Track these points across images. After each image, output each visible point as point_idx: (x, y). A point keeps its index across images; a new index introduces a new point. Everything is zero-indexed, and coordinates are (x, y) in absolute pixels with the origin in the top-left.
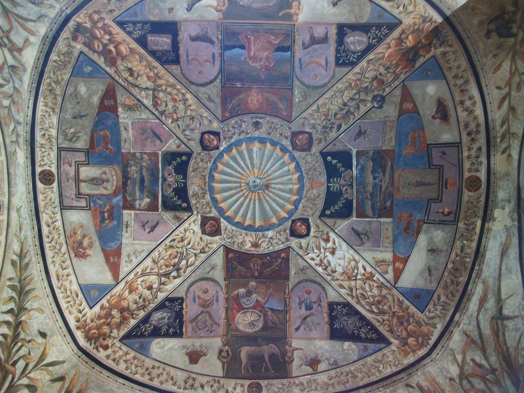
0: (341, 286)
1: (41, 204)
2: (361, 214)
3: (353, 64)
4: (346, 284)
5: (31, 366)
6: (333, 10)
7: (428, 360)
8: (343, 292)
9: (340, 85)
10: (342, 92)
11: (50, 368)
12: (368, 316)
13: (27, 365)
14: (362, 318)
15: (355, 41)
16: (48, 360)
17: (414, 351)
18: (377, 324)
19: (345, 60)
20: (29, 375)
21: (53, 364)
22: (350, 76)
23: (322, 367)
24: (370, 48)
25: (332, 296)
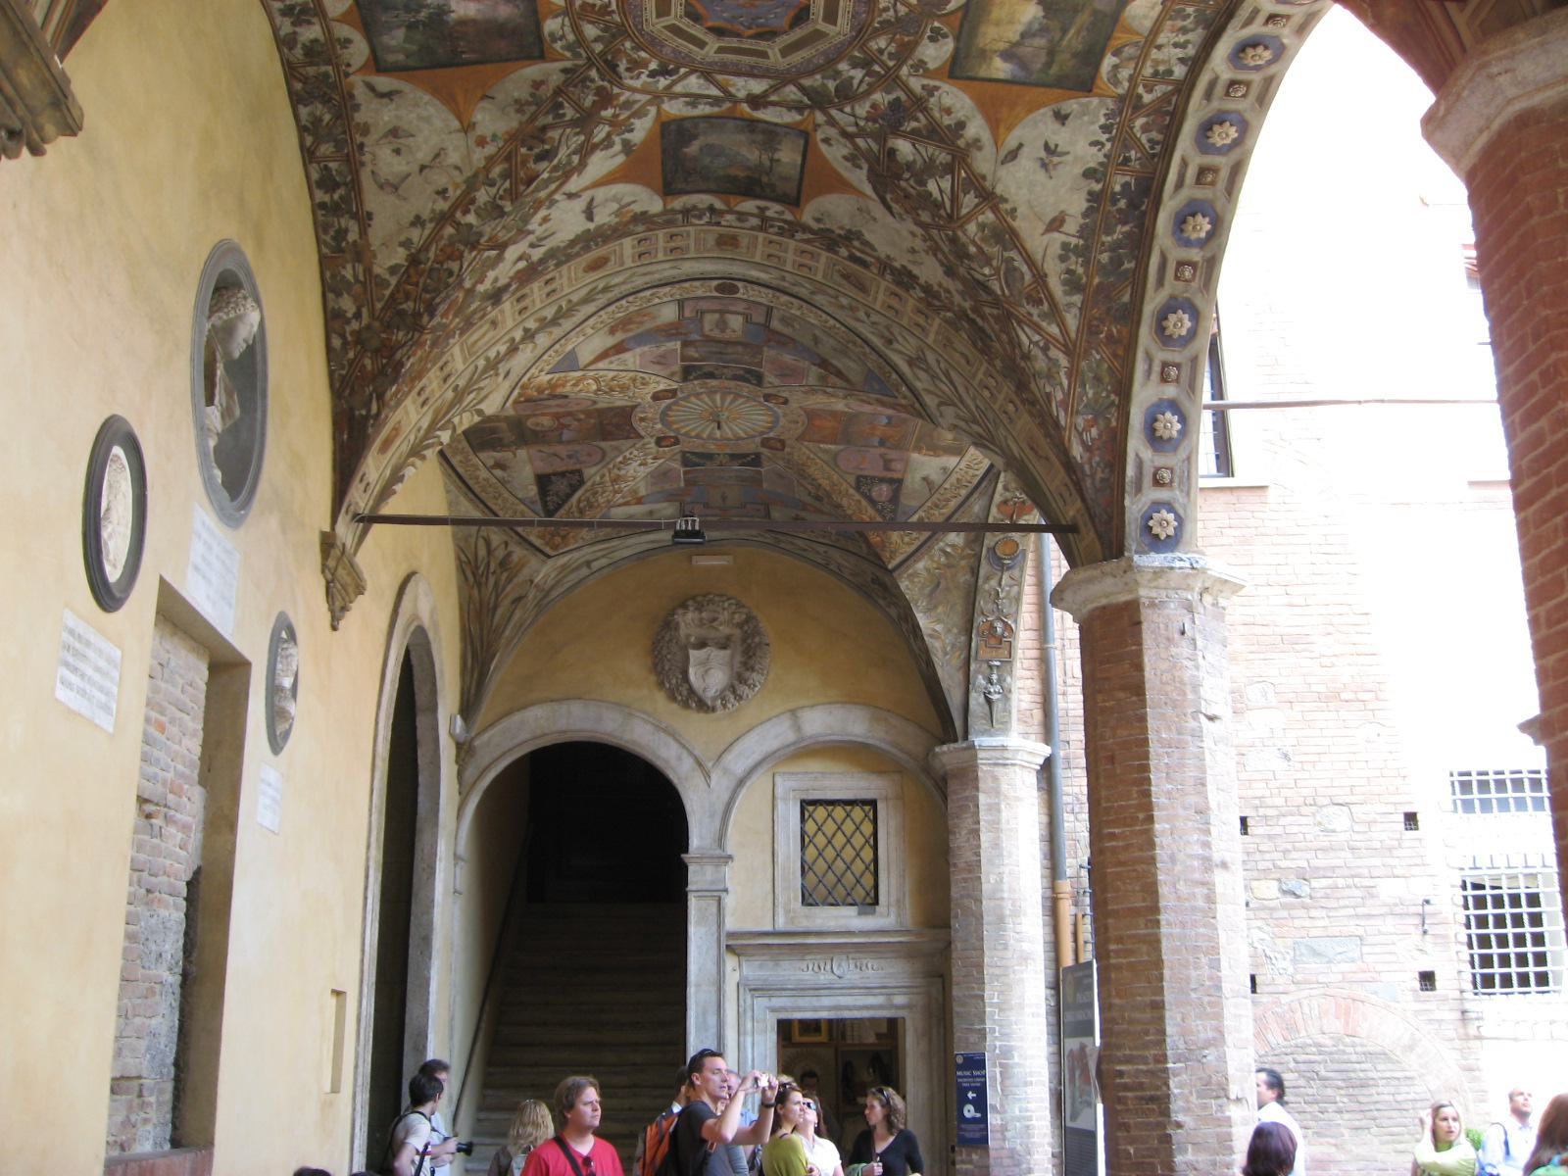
0: (603, 476)
1: (687, 285)
2: (685, 473)
3: (858, 488)
4: (607, 478)
6: (918, 477)
7: (543, 557)
8: (597, 478)
9: (835, 477)
10: (828, 478)
12: (574, 500)
14: (569, 496)
15: (882, 492)
17: (547, 544)
18: (566, 507)
19: (862, 483)
22: (845, 485)
23: (498, 472)
24: (873, 502)
25: (589, 472)
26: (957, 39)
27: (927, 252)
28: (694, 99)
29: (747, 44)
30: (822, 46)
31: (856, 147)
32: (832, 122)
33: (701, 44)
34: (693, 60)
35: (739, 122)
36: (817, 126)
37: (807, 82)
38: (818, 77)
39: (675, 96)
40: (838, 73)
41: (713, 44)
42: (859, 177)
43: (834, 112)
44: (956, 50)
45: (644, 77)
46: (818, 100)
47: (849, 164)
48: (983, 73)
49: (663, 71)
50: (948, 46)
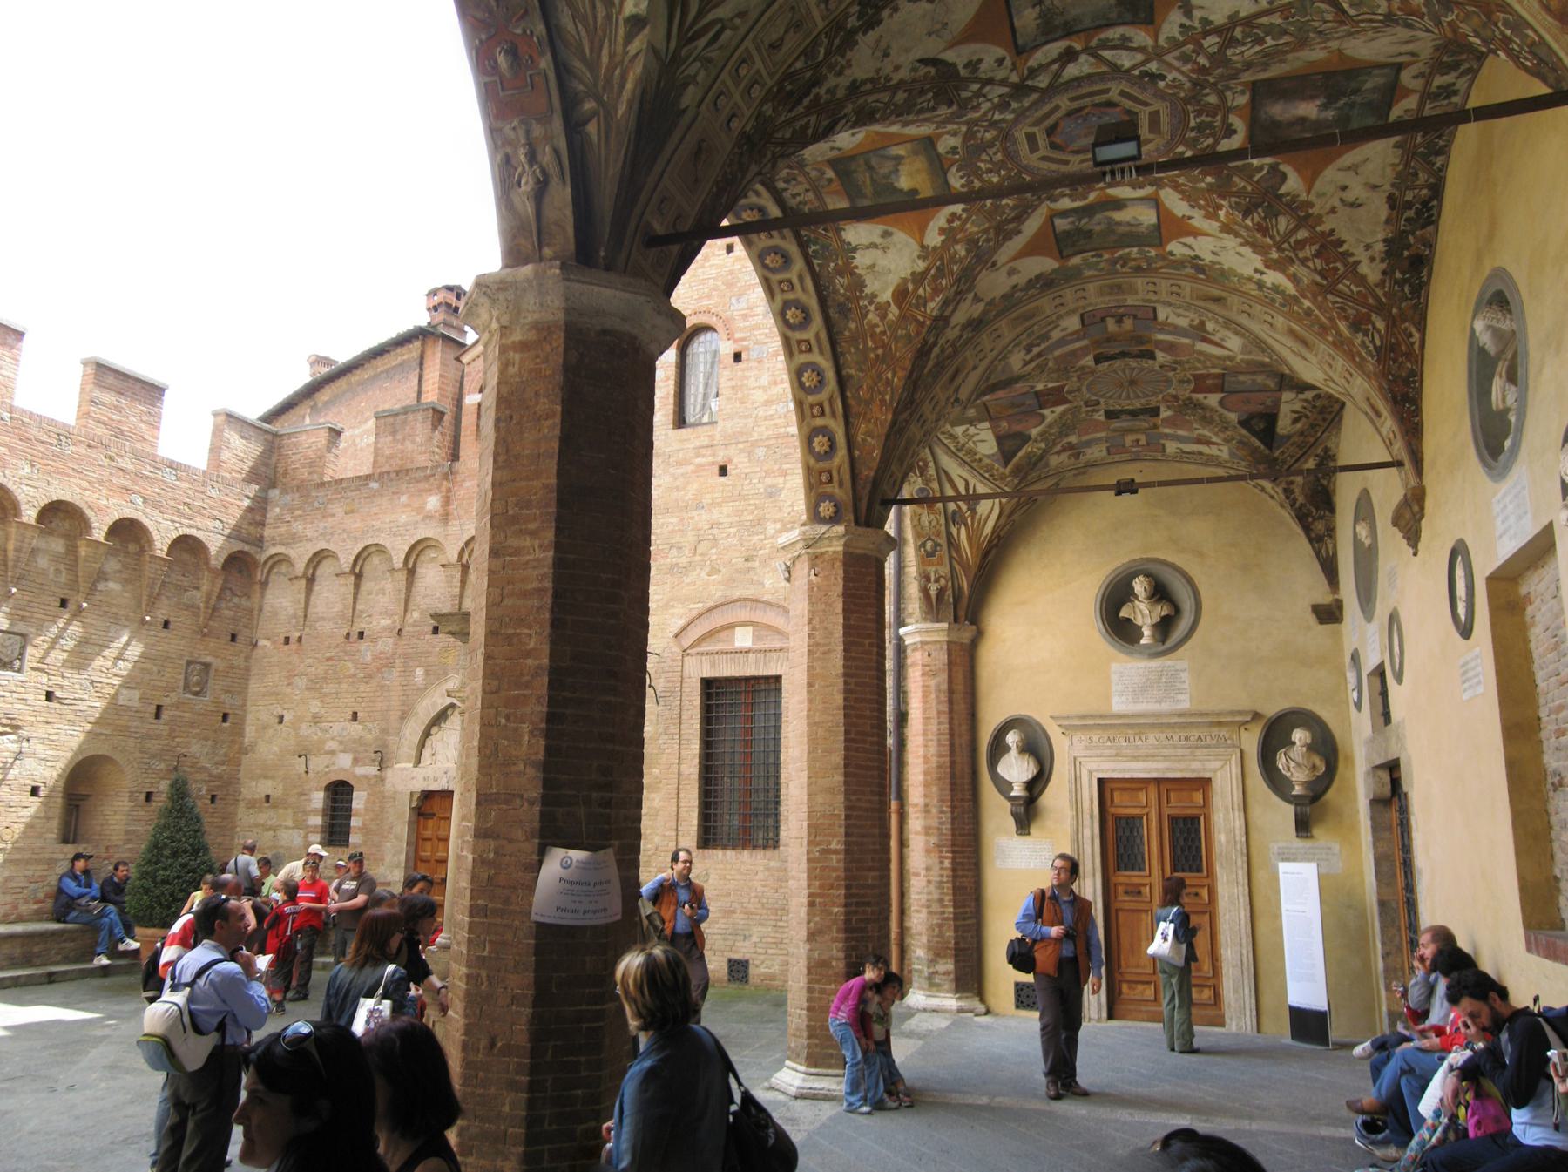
26: (938, 155)
27: (878, 71)
28: (1124, 44)
29: (1087, 101)
30: (1030, 120)
31: (977, 80)
32: (1003, 82)
33: (1123, 94)
34: (1129, 80)
35: (1080, 27)
36: (1014, 68)
37: (1035, 96)
38: (1026, 104)
39: (1141, 49)
40: (1014, 111)
41: (1114, 95)
42: (957, 57)
43: (1005, 90)
44: (935, 150)
45: (1170, 77)
46: (1020, 90)
47: (975, 58)
48: (908, 145)
49: (1155, 77)
50: (941, 149)
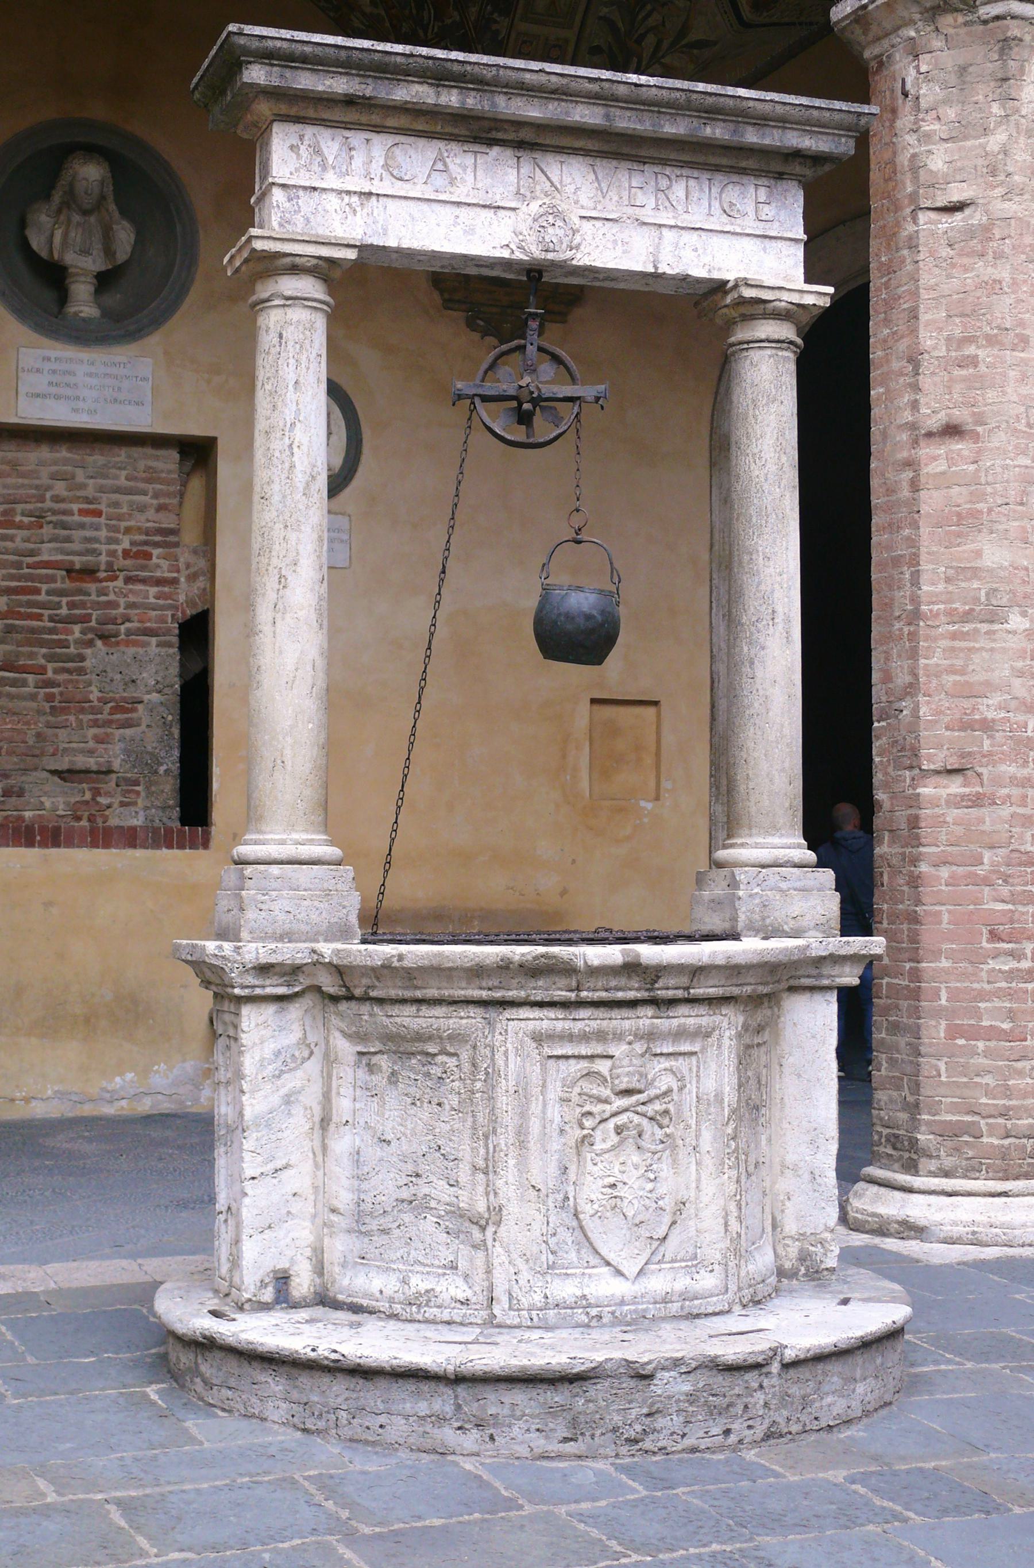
5: (665, 44)
11: (695, 51)
13: (660, 42)
16: (693, 36)
20: (663, 60)
21: (700, 44)
